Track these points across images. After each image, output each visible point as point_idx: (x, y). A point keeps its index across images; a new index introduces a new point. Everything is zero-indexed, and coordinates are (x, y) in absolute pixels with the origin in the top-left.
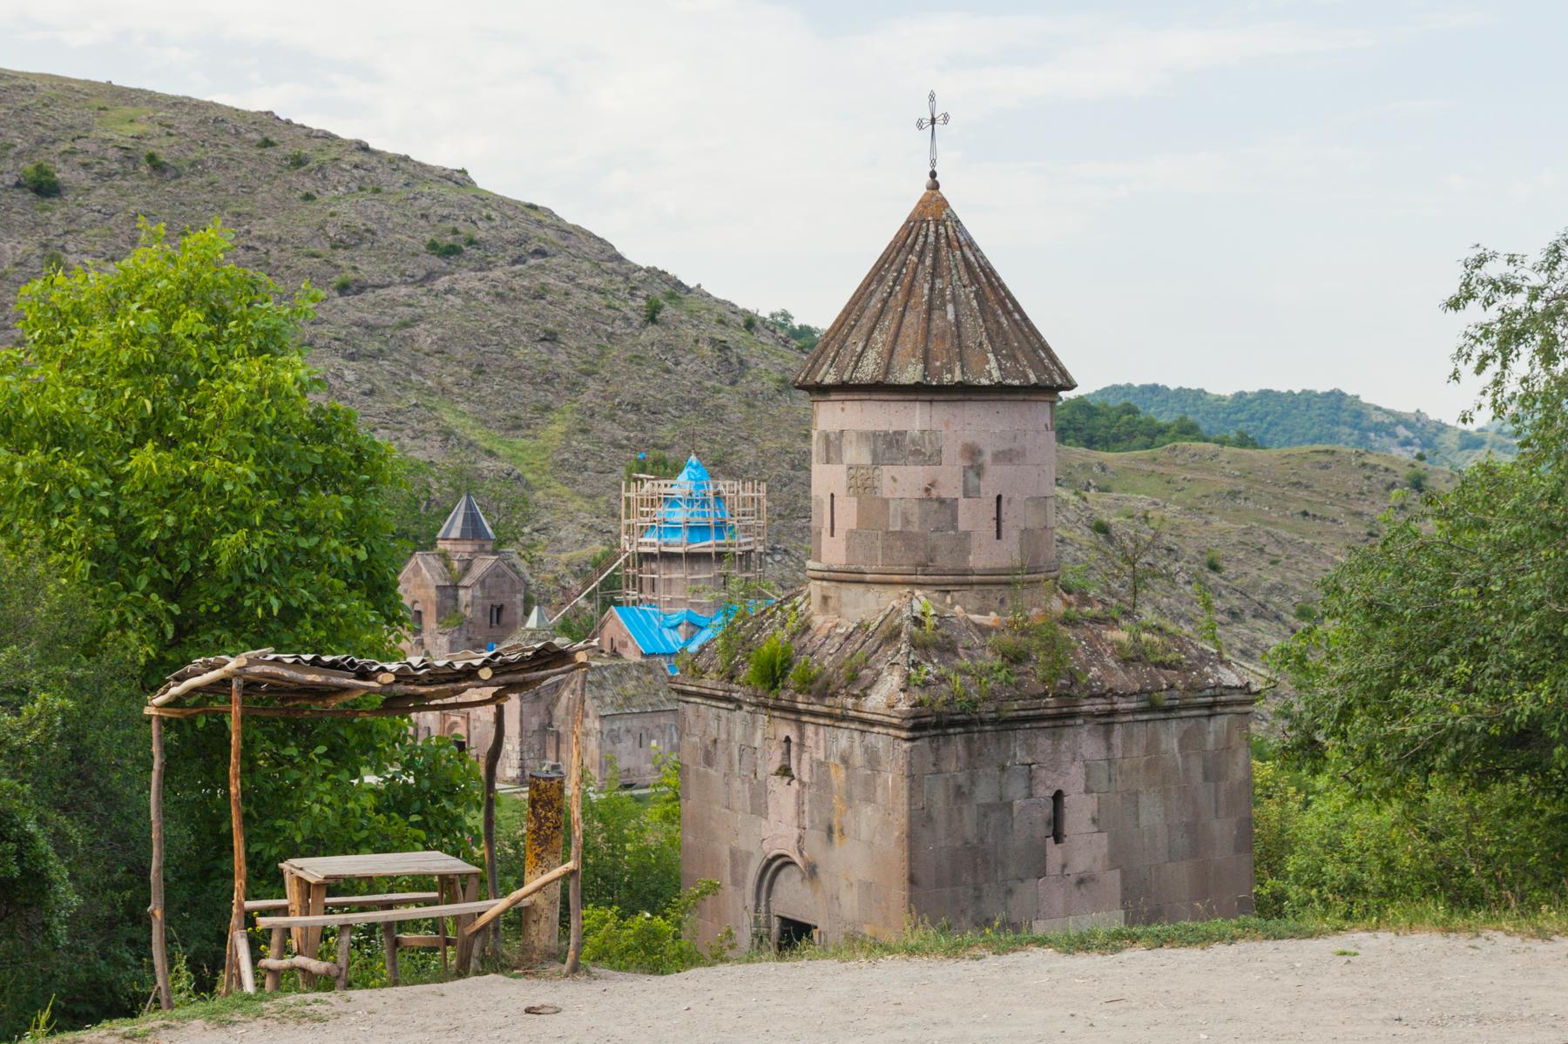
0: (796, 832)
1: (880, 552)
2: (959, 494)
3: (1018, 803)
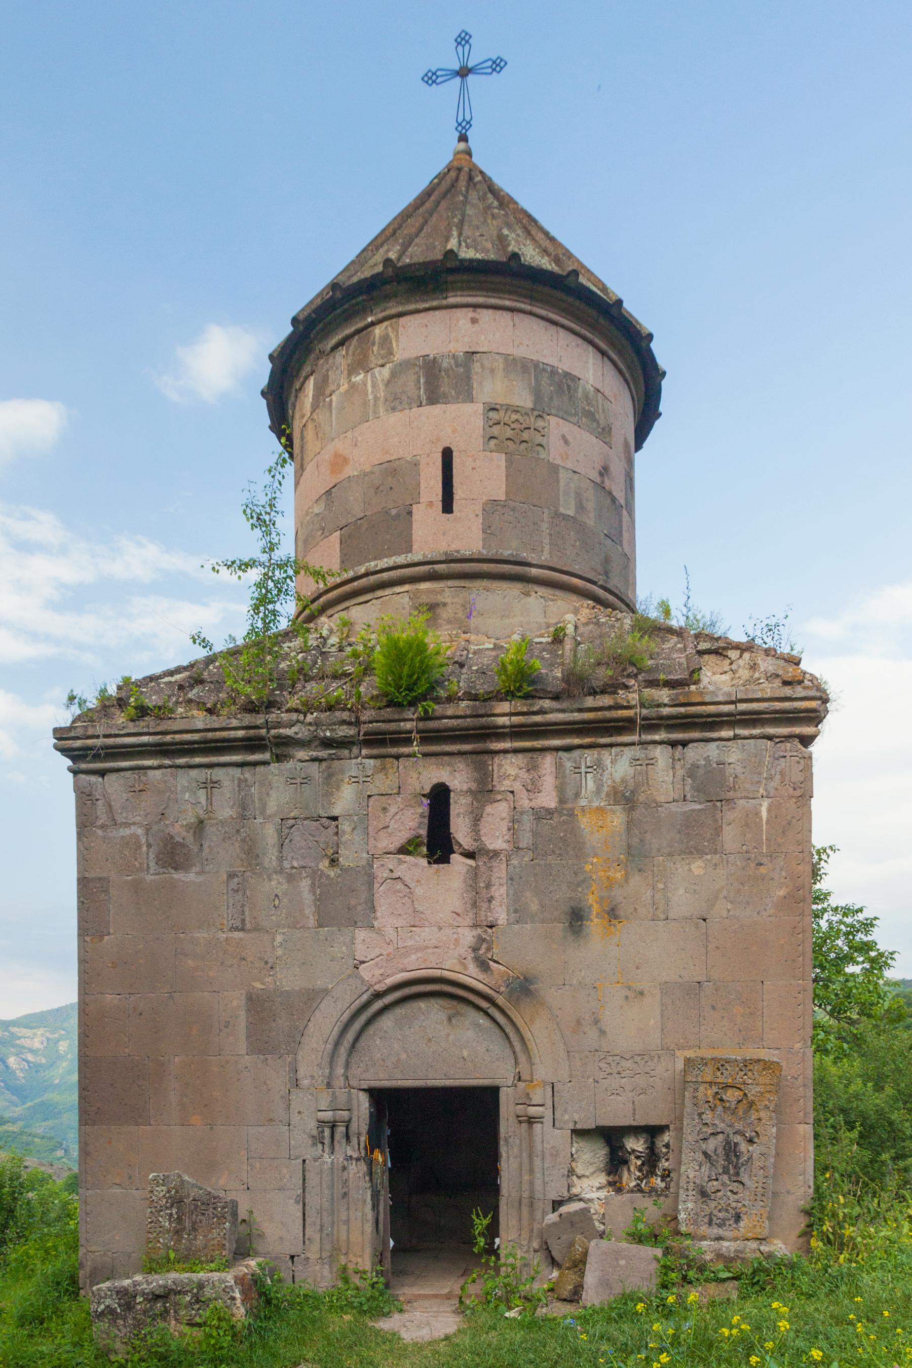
0: (468, 936)
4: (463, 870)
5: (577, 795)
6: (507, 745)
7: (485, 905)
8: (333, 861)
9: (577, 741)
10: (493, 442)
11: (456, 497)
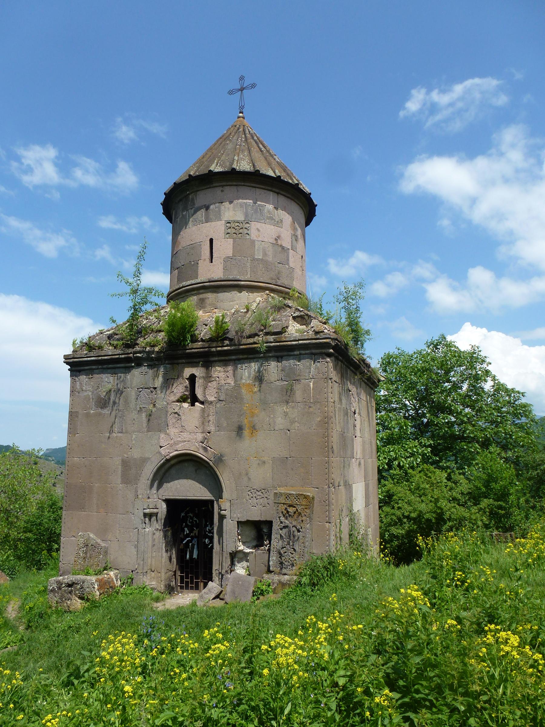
0: (200, 437)
1: (249, 270)
2: (290, 247)
4: (199, 409)
5: (241, 378)
6: (217, 359)
7: (207, 424)
8: (154, 405)
9: (241, 357)
10: (228, 235)
11: (214, 257)
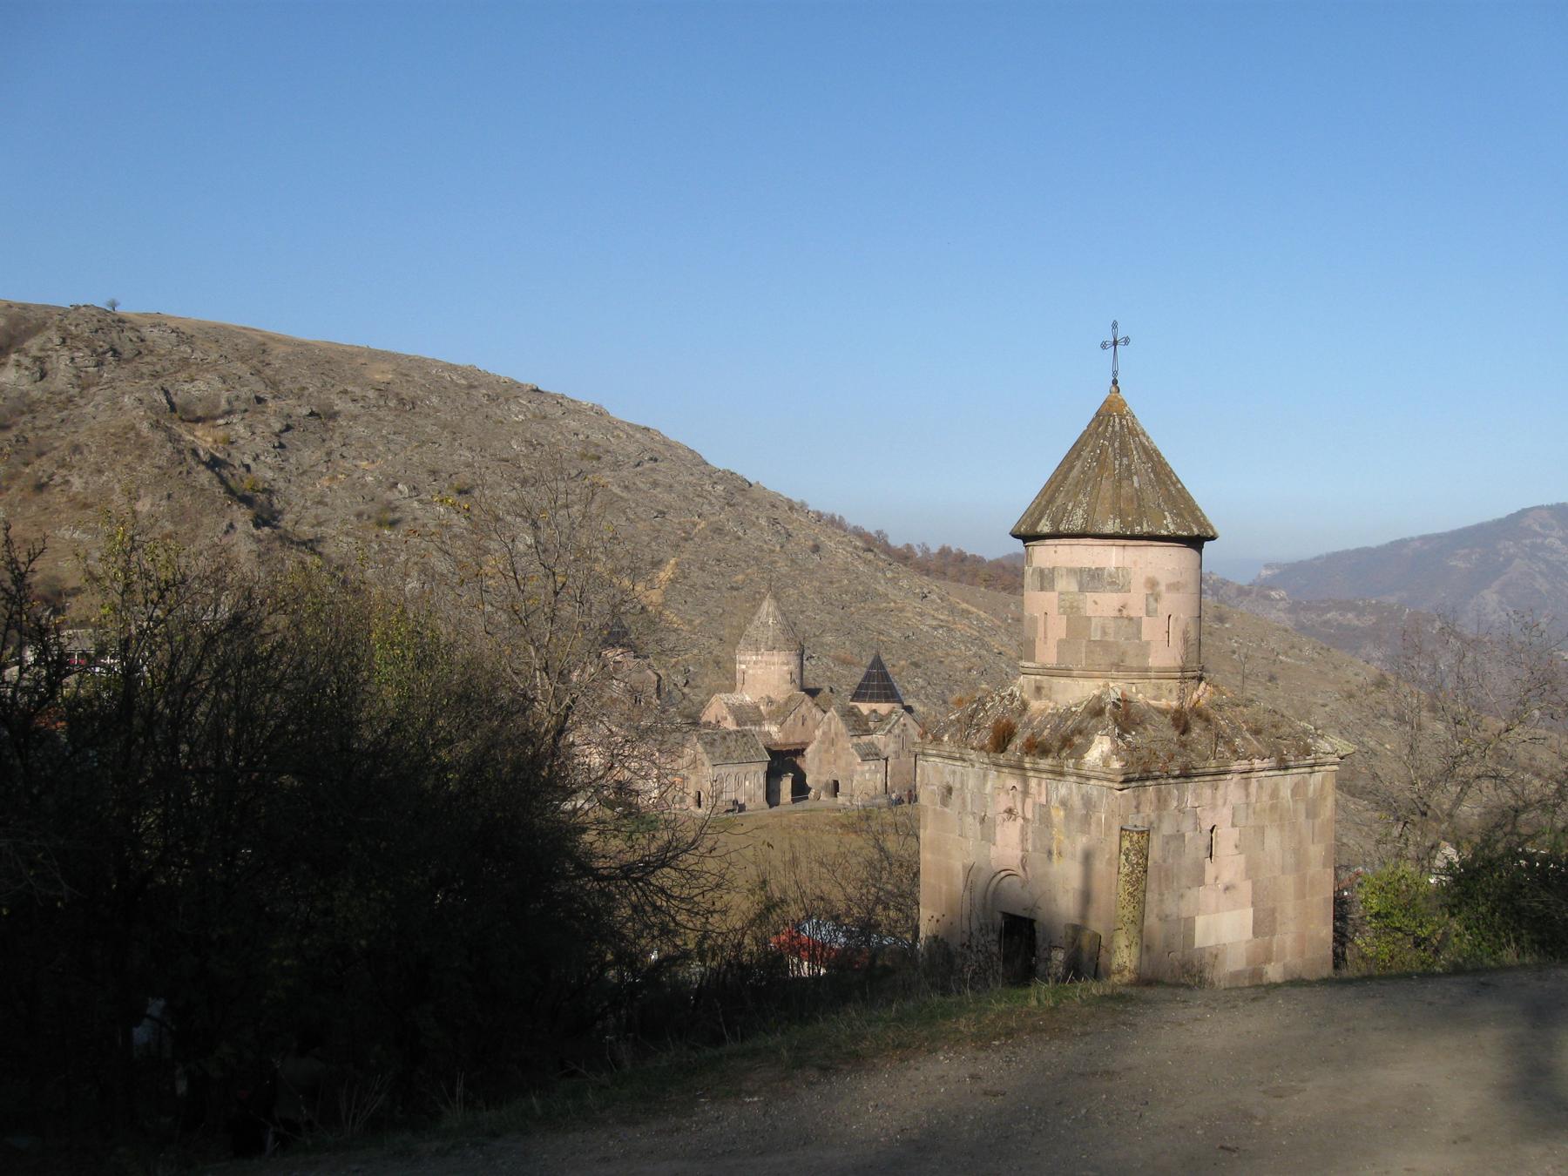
0: (1020, 854)
2: (1142, 614)
3: (1188, 835)
